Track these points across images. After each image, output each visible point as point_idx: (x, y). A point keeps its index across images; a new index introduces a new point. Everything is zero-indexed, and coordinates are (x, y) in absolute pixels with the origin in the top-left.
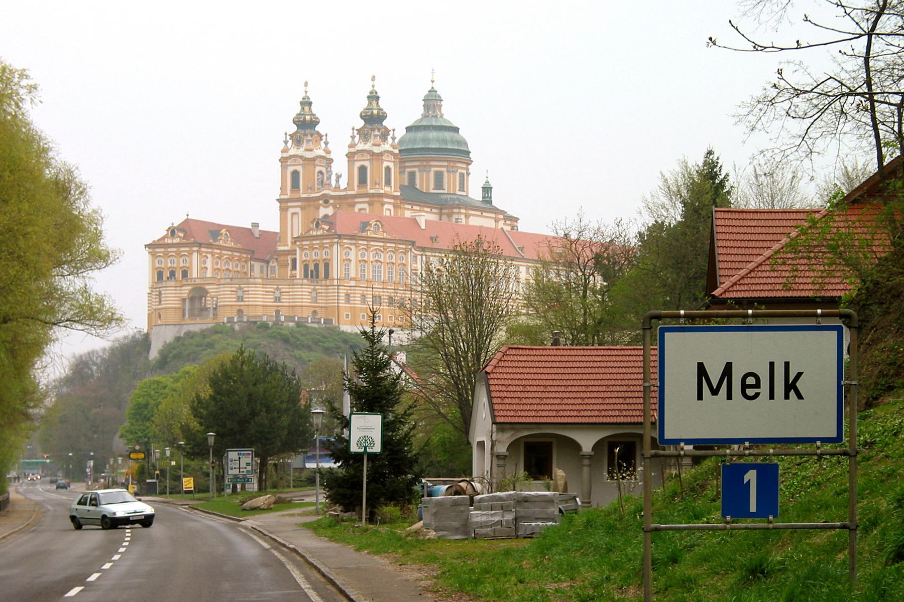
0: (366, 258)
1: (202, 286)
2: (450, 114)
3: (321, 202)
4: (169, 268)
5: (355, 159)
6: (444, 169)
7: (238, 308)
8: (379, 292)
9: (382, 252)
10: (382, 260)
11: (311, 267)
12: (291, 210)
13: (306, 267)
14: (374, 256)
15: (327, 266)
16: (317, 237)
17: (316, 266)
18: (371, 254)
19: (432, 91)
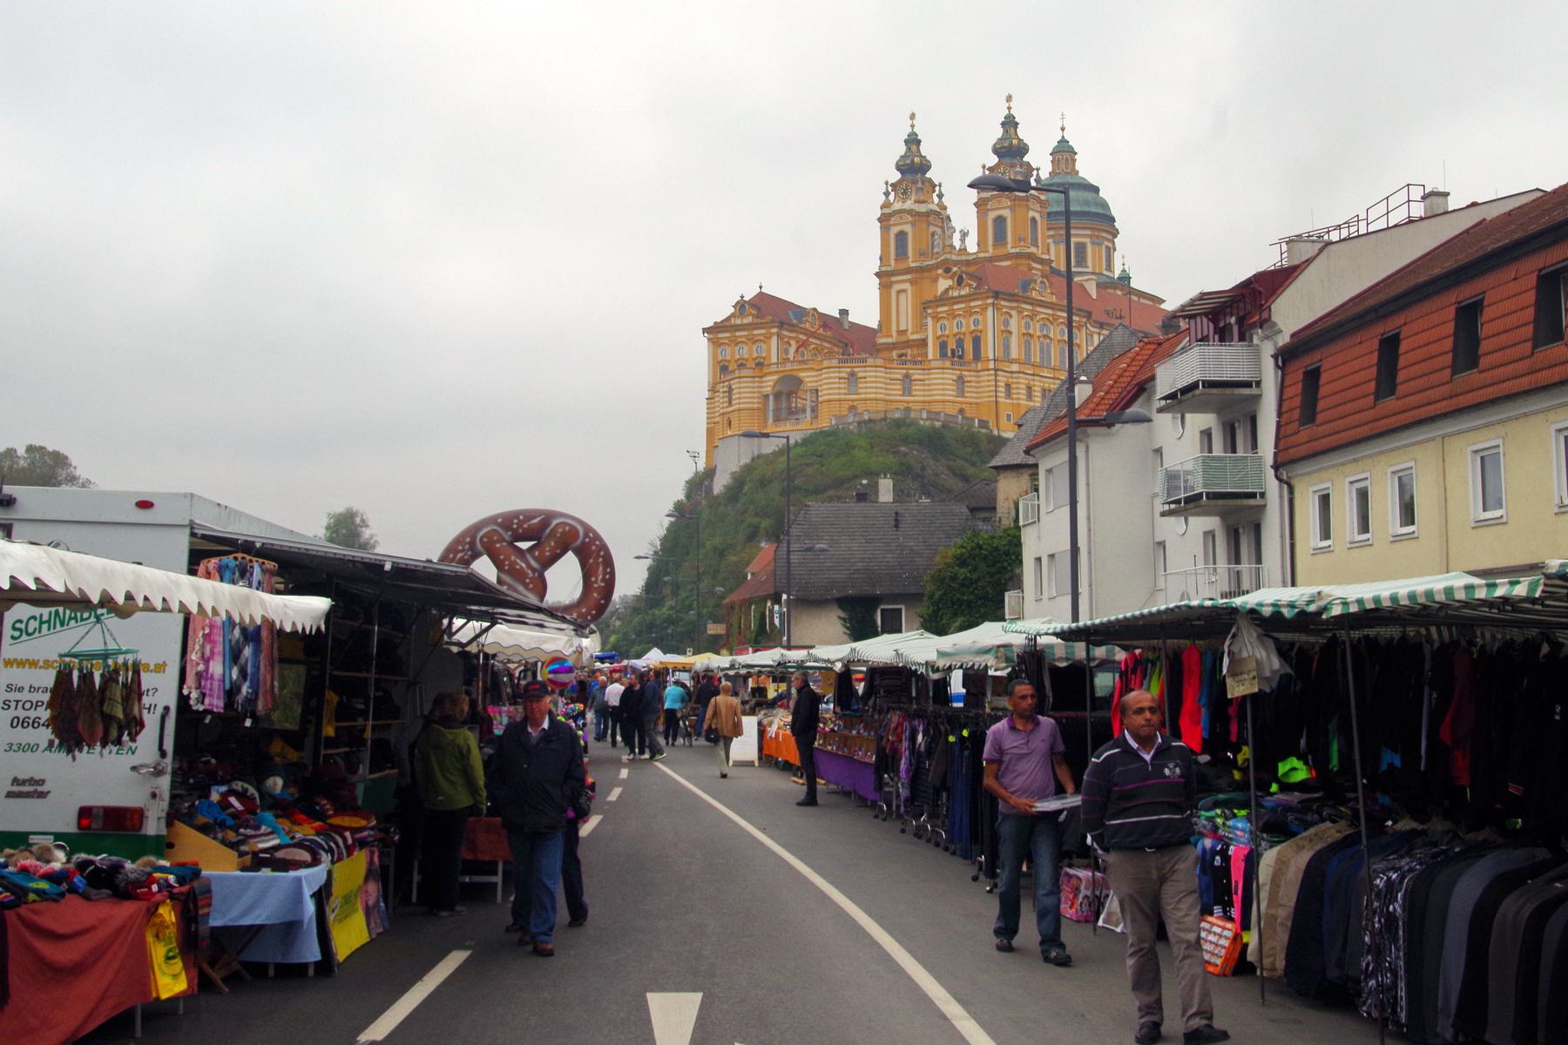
0: (1031, 331)
1: (794, 373)
2: (1086, 170)
3: (940, 271)
4: (736, 361)
5: (989, 207)
6: (1087, 240)
7: (851, 403)
8: (1049, 384)
9: (1052, 324)
10: (1051, 335)
11: (952, 345)
12: (897, 287)
13: (943, 346)
14: (1041, 331)
15: (977, 342)
16: (960, 299)
17: (960, 343)
18: (1038, 325)
19: (1063, 141)
